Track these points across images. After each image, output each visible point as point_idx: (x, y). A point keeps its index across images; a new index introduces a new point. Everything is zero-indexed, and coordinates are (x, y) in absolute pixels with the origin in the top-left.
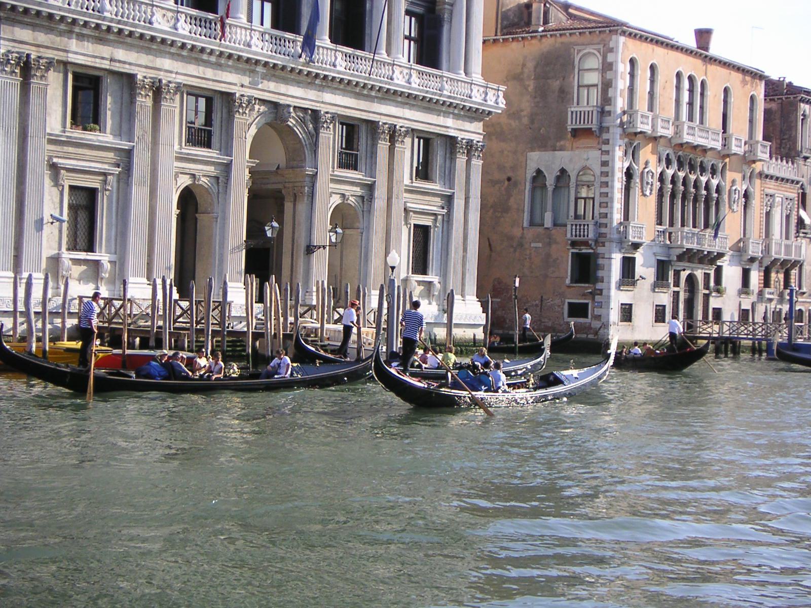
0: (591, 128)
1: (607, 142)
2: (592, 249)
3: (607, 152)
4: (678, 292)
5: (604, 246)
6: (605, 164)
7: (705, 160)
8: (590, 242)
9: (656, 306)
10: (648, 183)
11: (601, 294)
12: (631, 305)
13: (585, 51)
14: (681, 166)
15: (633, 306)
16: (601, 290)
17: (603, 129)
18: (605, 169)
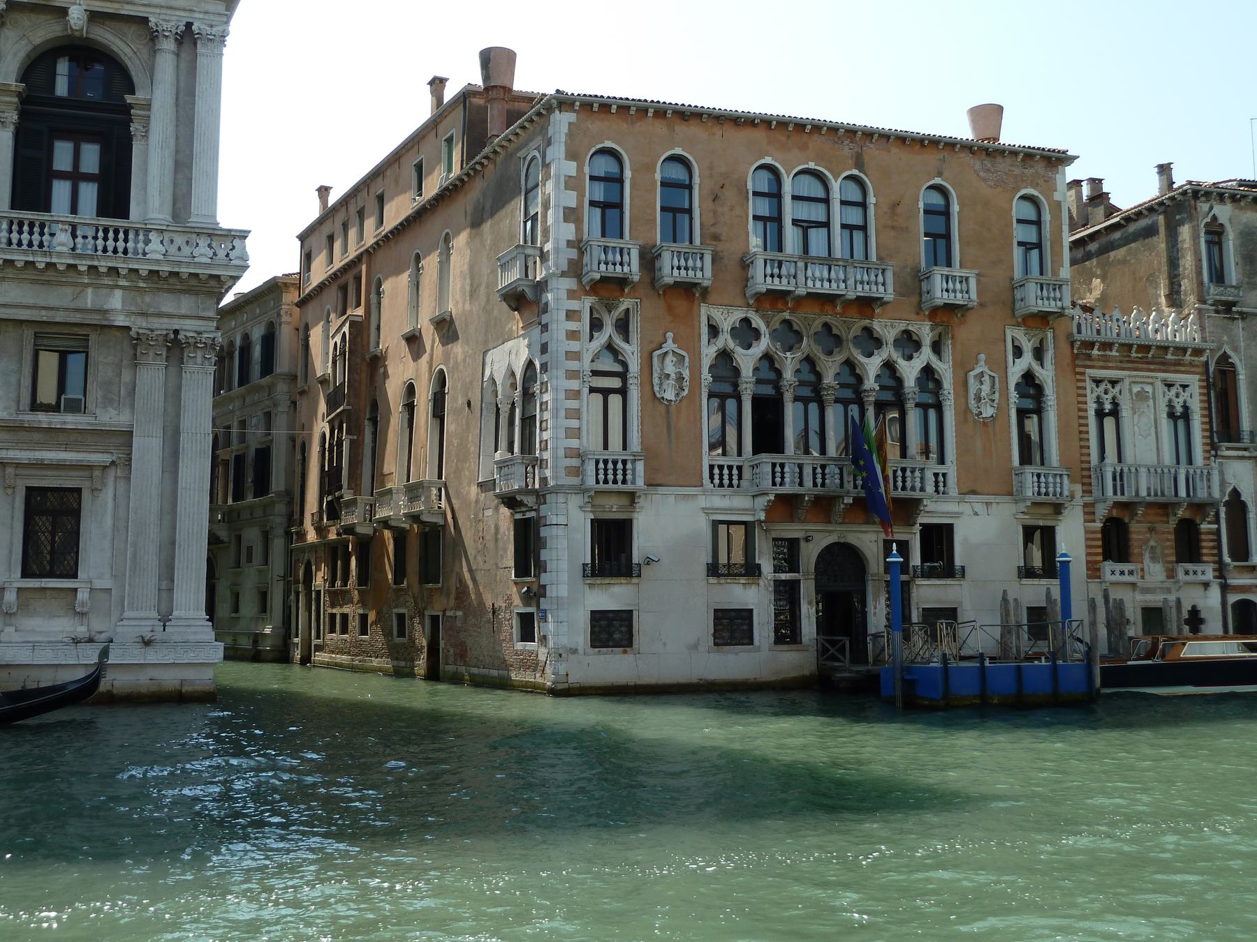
0: (516, 288)
1: (545, 310)
2: (531, 509)
3: (545, 328)
4: (795, 585)
5: (545, 503)
6: (544, 349)
7: (877, 326)
8: (518, 498)
9: (716, 611)
10: (668, 376)
11: (544, 596)
12: (631, 612)
13: (529, 158)
14: (789, 335)
15: (635, 614)
16: (544, 587)
17: (541, 287)
18: (546, 358)
